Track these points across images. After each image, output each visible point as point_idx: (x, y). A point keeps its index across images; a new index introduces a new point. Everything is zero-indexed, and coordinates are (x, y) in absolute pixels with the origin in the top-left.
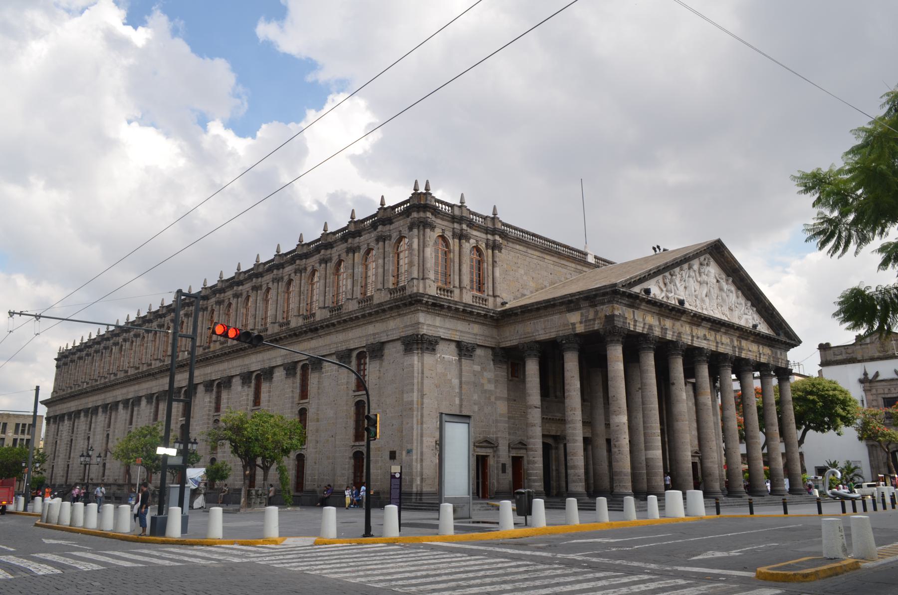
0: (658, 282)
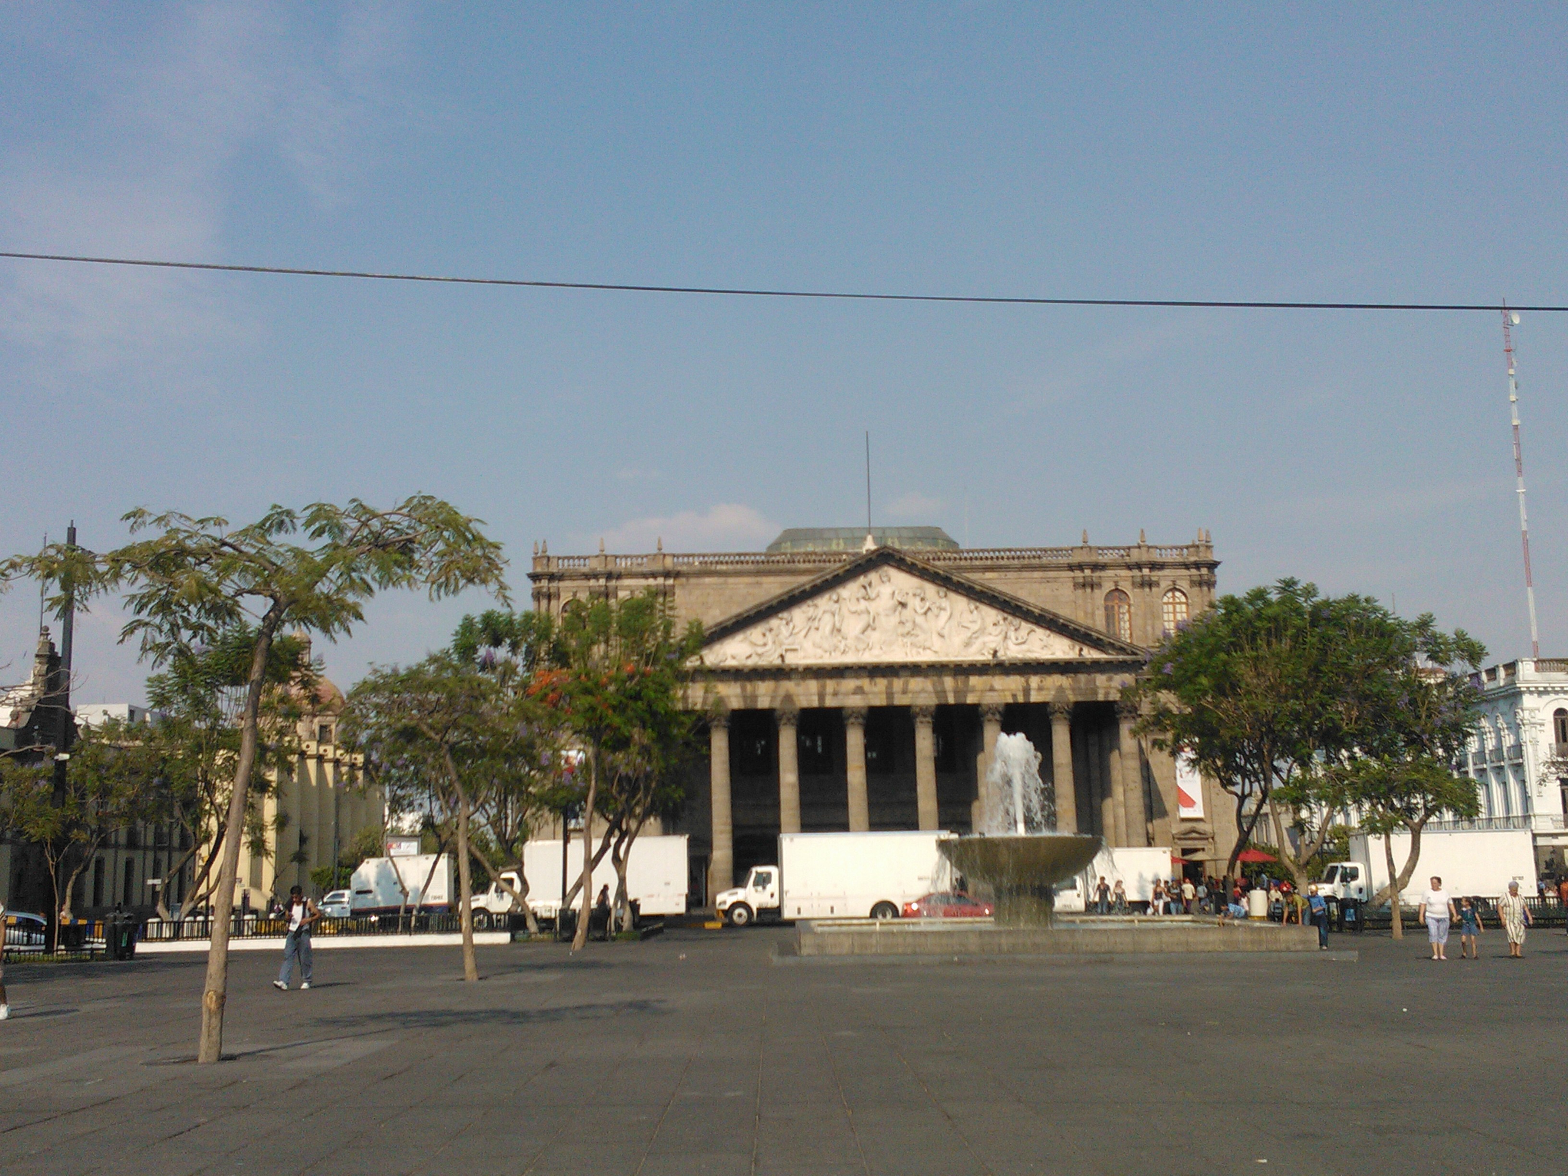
0: (745, 638)
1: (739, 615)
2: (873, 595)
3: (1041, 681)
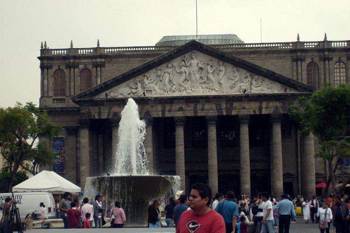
1: (124, 74)
2: (188, 65)
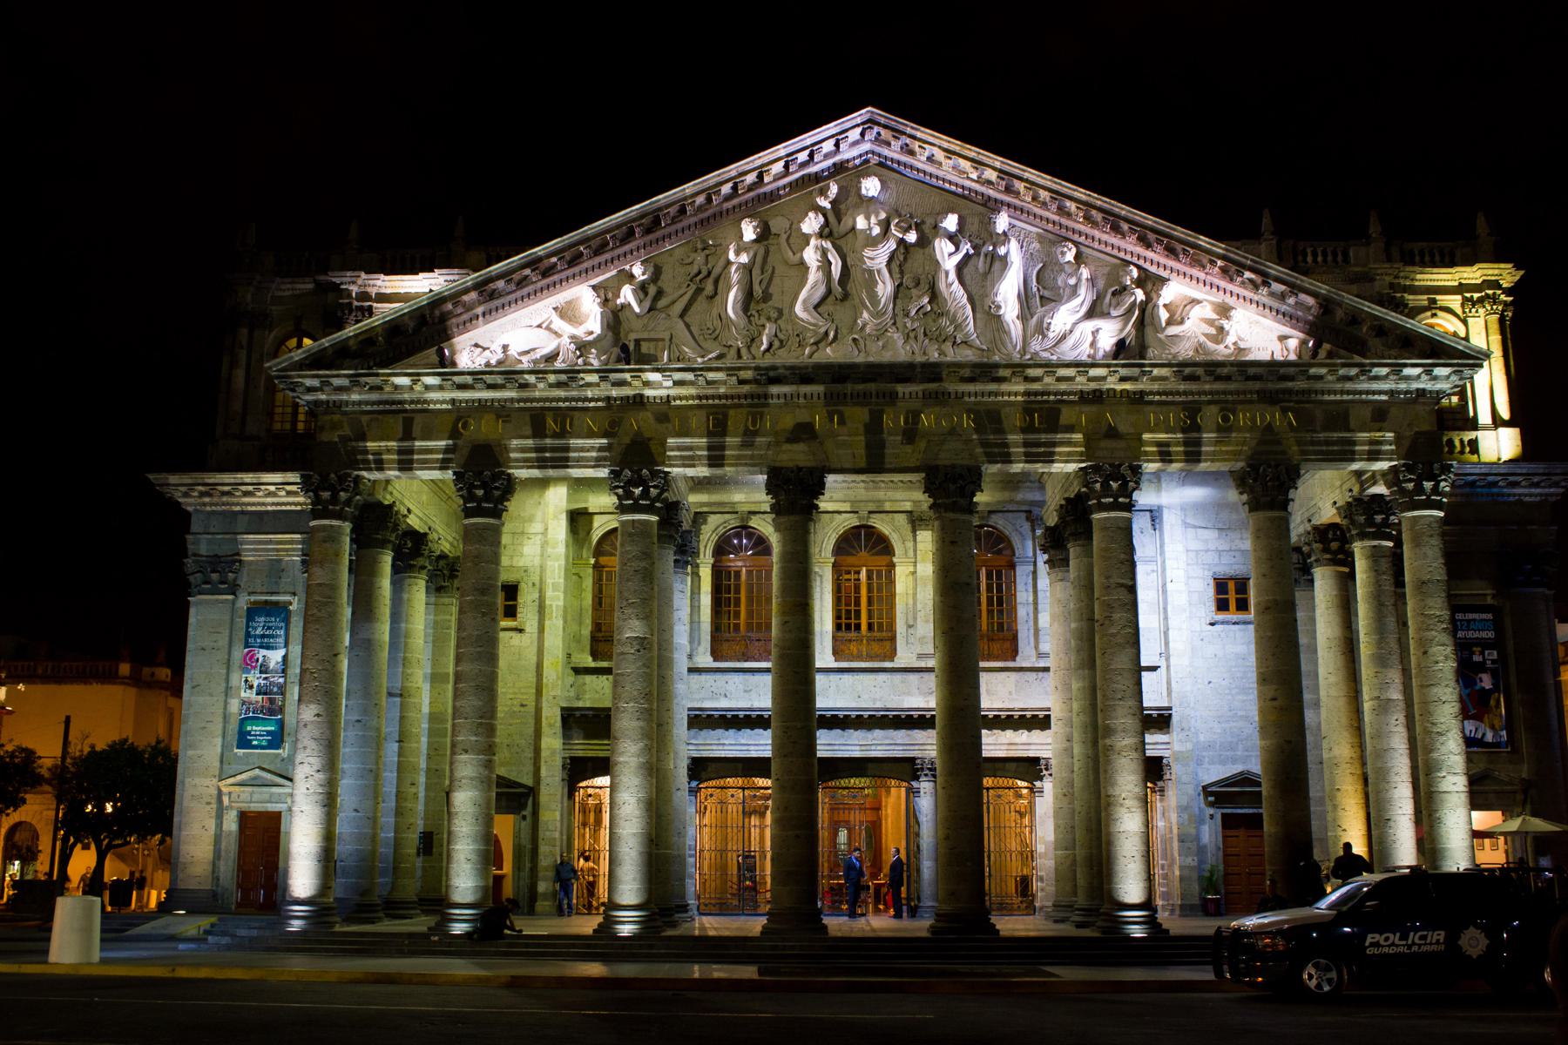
3: (1226, 419)
